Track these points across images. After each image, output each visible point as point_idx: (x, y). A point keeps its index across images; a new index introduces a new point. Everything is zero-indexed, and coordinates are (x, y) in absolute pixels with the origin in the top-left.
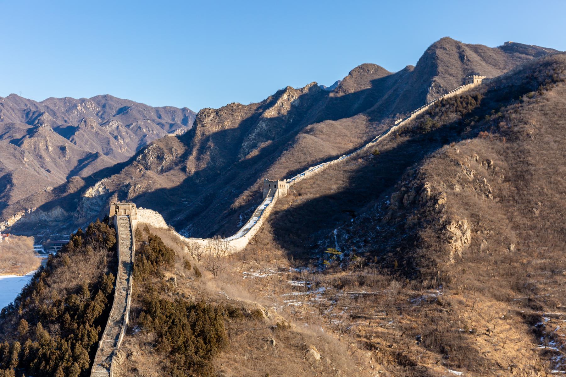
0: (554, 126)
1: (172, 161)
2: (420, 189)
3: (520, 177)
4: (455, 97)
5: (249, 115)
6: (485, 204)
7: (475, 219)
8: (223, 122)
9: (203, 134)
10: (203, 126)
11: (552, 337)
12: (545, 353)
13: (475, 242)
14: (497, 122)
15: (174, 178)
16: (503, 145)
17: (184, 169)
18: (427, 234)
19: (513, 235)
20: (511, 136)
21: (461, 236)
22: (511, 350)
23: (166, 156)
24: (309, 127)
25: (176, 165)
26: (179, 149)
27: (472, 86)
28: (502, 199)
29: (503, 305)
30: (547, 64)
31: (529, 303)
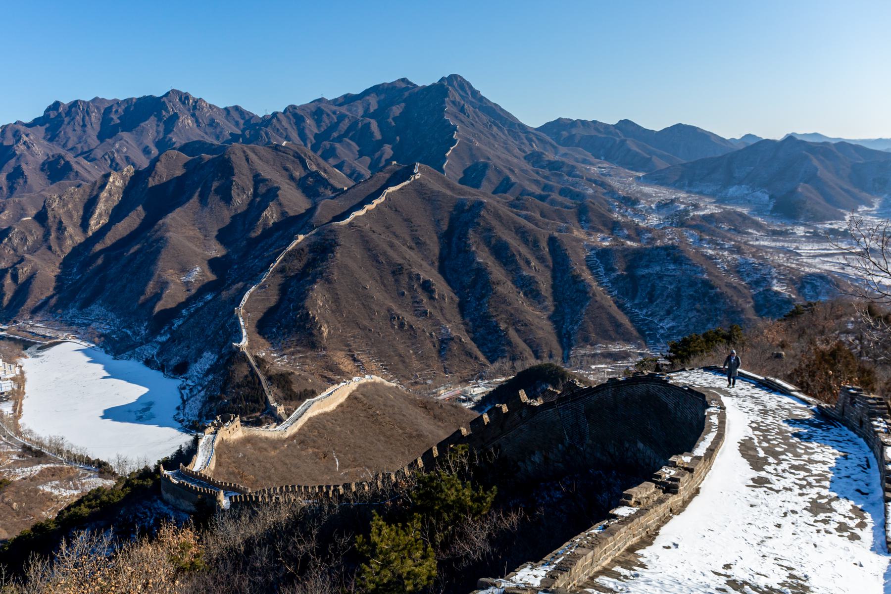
0: (343, 274)
1: (34, 241)
2: (308, 314)
3: (336, 300)
4: (293, 249)
5: (86, 197)
6: (328, 314)
7: (327, 322)
8: (67, 205)
9: (55, 217)
10: (53, 210)
11: (358, 361)
12: (358, 366)
13: (329, 332)
14: (321, 273)
15: (45, 257)
16: (327, 285)
17: (50, 248)
18: (315, 332)
19: (339, 325)
20: (329, 281)
21: (325, 330)
22: (350, 367)
23: (28, 238)
24: (160, 222)
25: (41, 245)
26: (37, 232)
27: (299, 241)
28: (333, 312)
29: (343, 352)
30: (331, 231)
31: (350, 351)
